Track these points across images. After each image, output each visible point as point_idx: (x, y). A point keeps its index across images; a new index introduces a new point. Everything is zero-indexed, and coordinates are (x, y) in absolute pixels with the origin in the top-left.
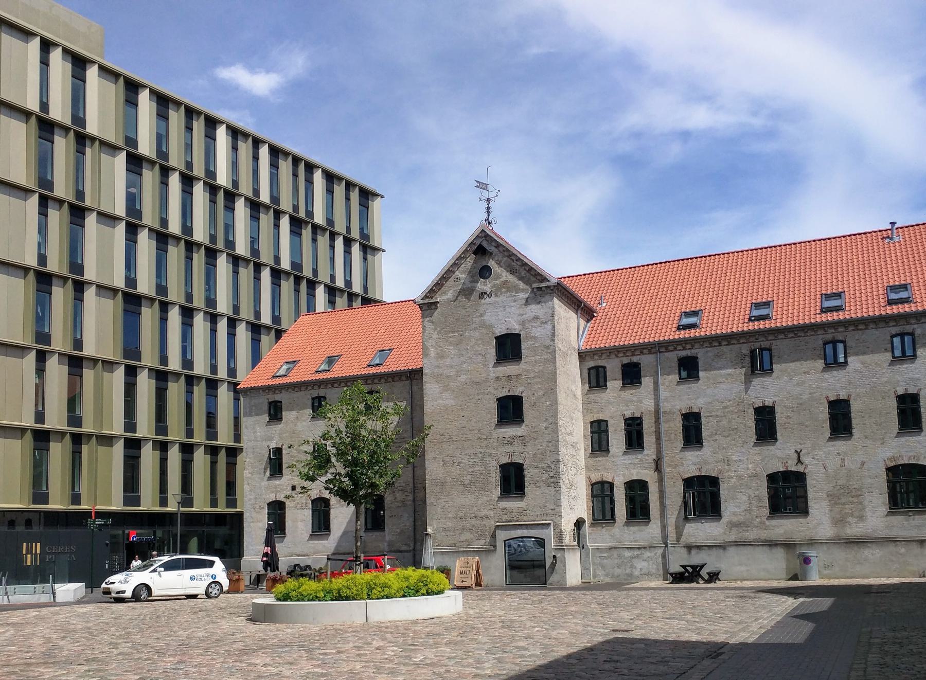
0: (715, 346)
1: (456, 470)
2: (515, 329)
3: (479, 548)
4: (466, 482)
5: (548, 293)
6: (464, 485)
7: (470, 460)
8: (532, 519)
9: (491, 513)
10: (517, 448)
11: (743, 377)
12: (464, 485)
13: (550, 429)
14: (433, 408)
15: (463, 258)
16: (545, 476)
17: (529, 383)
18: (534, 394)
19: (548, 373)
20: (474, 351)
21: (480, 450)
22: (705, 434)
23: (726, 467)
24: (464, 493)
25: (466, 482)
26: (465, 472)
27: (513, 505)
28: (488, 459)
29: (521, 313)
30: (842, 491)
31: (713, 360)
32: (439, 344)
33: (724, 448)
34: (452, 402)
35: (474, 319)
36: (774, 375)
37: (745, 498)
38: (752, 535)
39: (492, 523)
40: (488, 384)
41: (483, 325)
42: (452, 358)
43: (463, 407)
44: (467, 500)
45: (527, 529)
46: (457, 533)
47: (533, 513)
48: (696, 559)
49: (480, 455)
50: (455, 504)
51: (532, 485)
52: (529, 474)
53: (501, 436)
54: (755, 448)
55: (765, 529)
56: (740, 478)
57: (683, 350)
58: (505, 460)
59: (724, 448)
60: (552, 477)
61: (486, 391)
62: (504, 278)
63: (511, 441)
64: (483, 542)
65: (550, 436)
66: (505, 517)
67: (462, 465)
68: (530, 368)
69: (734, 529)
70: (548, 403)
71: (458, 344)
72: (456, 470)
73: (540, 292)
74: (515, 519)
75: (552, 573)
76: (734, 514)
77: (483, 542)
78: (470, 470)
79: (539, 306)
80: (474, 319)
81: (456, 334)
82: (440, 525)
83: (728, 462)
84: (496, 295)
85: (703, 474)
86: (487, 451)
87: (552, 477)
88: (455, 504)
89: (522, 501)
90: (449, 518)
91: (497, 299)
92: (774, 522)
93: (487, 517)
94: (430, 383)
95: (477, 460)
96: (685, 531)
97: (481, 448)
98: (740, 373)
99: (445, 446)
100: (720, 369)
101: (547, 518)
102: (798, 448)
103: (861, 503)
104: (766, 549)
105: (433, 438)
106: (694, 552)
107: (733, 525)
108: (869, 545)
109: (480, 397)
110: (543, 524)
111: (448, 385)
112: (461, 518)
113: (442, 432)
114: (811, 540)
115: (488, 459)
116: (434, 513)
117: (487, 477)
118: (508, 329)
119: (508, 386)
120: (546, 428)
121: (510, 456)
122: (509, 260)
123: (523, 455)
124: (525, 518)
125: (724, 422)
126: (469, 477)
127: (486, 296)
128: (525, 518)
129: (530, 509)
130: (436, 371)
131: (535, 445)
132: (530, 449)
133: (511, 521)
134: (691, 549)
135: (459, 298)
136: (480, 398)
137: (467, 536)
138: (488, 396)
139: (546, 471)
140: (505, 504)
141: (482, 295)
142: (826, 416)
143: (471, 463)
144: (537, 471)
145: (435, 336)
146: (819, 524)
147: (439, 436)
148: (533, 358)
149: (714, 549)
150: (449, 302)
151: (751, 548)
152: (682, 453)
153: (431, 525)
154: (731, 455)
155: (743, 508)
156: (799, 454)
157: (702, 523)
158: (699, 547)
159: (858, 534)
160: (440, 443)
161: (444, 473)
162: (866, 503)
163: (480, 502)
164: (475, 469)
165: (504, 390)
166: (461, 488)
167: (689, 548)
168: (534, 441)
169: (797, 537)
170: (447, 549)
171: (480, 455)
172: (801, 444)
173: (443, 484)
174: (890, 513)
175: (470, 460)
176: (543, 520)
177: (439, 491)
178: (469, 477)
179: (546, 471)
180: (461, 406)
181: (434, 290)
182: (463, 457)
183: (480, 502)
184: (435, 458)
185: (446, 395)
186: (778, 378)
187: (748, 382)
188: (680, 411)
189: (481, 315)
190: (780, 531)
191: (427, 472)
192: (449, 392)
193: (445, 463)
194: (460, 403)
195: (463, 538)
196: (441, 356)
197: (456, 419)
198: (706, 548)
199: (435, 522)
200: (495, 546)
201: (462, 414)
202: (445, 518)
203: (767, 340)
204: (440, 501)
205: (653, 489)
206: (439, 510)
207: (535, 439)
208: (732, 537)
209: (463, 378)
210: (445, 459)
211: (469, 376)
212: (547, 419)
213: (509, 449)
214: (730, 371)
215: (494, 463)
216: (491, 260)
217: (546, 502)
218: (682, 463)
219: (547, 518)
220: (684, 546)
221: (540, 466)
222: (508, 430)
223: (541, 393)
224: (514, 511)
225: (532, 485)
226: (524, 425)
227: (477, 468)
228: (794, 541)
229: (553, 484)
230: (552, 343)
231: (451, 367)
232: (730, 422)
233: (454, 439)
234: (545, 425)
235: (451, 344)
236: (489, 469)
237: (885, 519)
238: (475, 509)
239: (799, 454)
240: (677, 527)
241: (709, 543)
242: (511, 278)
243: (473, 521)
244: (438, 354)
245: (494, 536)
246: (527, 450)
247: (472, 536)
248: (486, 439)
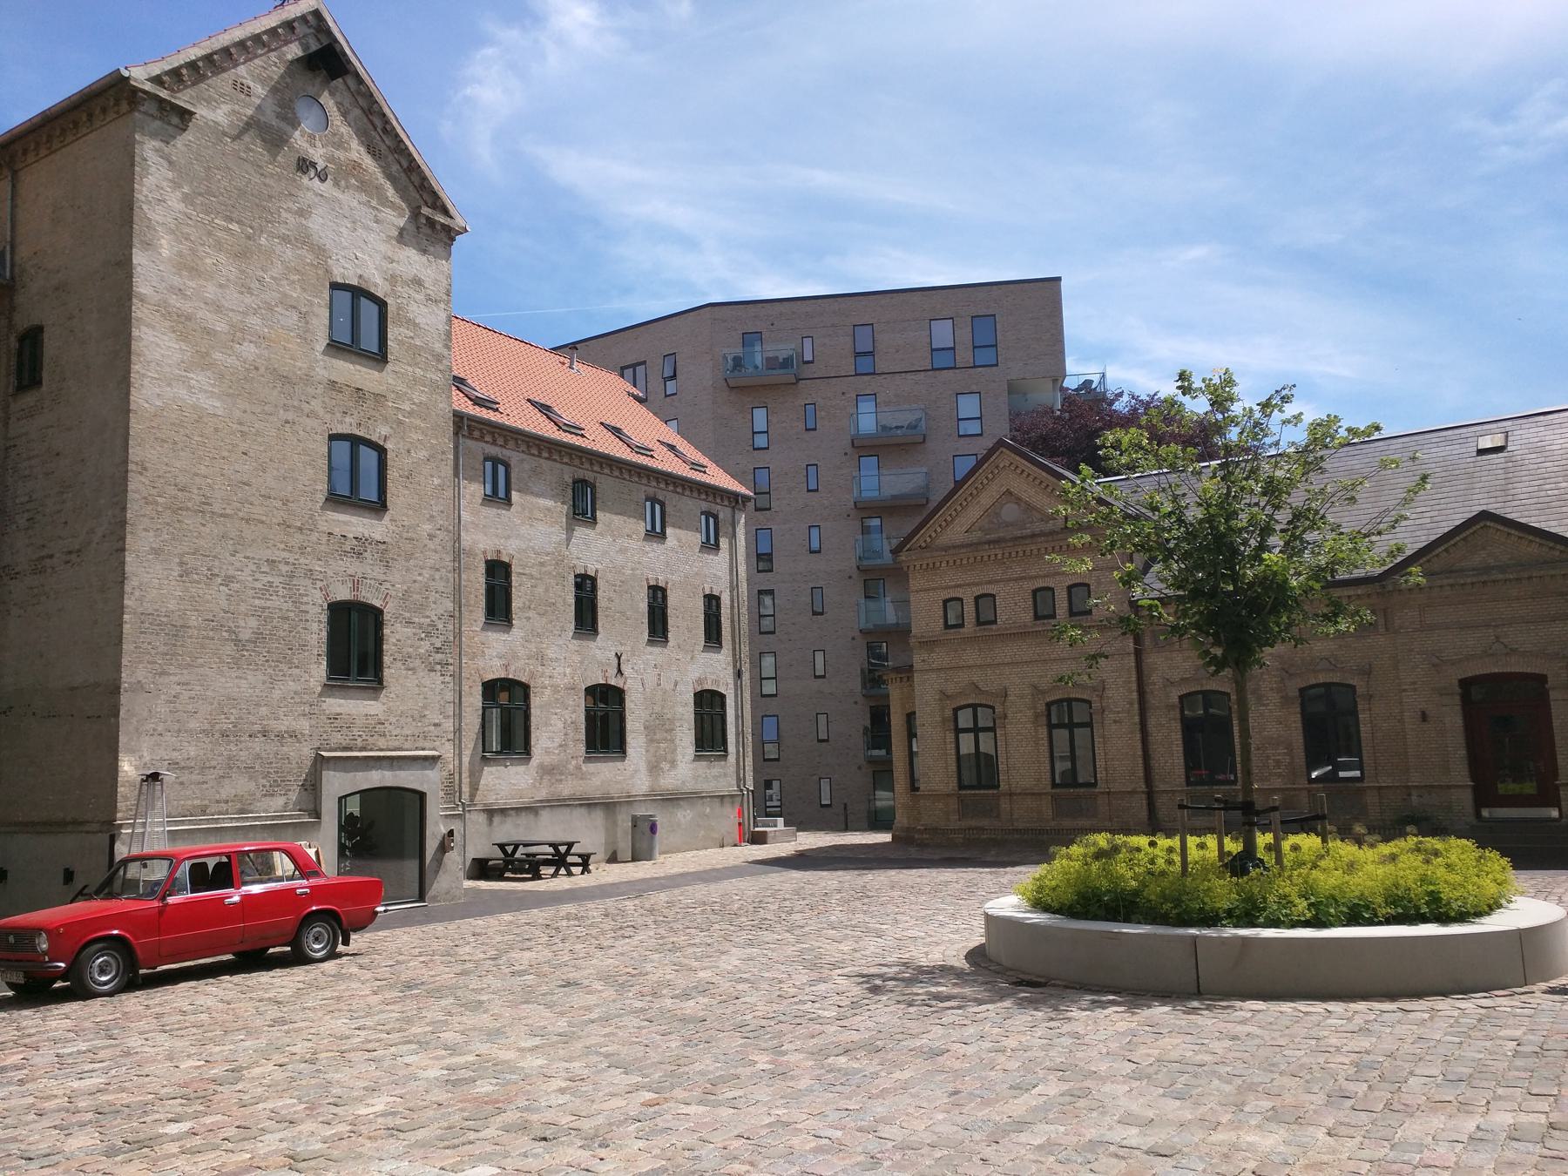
0: (533, 455)
1: (217, 597)
2: (376, 285)
3: (273, 818)
4: (245, 635)
5: (441, 240)
6: (237, 642)
7: (258, 576)
8: (396, 744)
9: (304, 725)
10: (369, 568)
11: (564, 520)
12: (237, 642)
13: (437, 541)
14: (159, 403)
15: (264, 45)
16: (425, 647)
17: (400, 423)
18: (409, 451)
19: (437, 415)
20: (279, 292)
21: (285, 555)
22: (516, 604)
23: (540, 668)
24: (236, 663)
25: (245, 635)
26: (243, 608)
27: (355, 707)
28: (303, 583)
29: (390, 254)
30: (657, 722)
31: (530, 477)
32: (187, 230)
33: (538, 635)
34: (218, 404)
35: (284, 214)
36: (599, 527)
37: (560, 725)
38: (567, 788)
39: (304, 753)
40: (310, 390)
41: (303, 239)
42: (221, 286)
43: (245, 429)
44: (247, 684)
45: (391, 768)
46: (211, 776)
47: (397, 731)
48: (509, 831)
49: (284, 568)
50: (209, 693)
51: (399, 664)
52: (395, 636)
53: (337, 531)
54: (575, 642)
55: (582, 779)
56: (555, 689)
57: (492, 444)
58: (343, 594)
59: (538, 635)
60: (438, 650)
61: (305, 406)
62: (354, 155)
63: (360, 547)
64: (279, 801)
65: (437, 557)
66: (337, 739)
67: (235, 586)
68: (401, 388)
69: (547, 777)
70: (436, 481)
71: (241, 255)
72: (217, 597)
73: (429, 231)
74: (359, 742)
75: (437, 872)
76: (547, 752)
77: (279, 801)
78: (257, 602)
79: (424, 259)
80: (284, 214)
81: (234, 227)
82: (162, 753)
83: (541, 658)
84: (336, 184)
85: (510, 677)
86: (302, 561)
87: (438, 650)
88: (209, 693)
89: (376, 699)
90: (190, 732)
91: (337, 193)
92: (592, 767)
93: (293, 735)
94: (153, 328)
95: (277, 580)
96: (482, 782)
97: (289, 549)
98: (561, 509)
99: (190, 521)
100: (537, 495)
101: (427, 745)
102: (620, 649)
103: (673, 741)
104: (583, 811)
105: (154, 492)
106: (497, 819)
107: (548, 771)
108: (682, 803)
109: (290, 416)
110: (426, 758)
111: (207, 354)
112: (224, 734)
113: (182, 480)
114: (629, 797)
115: (303, 583)
116: (145, 714)
117: (299, 629)
118: (360, 276)
119: (356, 413)
120: (431, 537)
121: (356, 586)
122: (365, 120)
123: (383, 588)
124: (382, 743)
125: (540, 590)
126: (253, 623)
127: (312, 173)
128: (382, 743)
129: (393, 720)
130: (174, 300)
131: (408, 570)
132: (398, 579)
133: (350, 749)
134: (492, 816)
135: (247, 138)
136: (290, 418)
137: (241, 785)
138: (308, 420)
139: (428, 634)
140: (339, 705)
141: (304, 165)
142: (646, 609)
143: (258, 585)
144: (409, 631)
145: (175, 201)
146: (636, 771)
147: (171, 490)
148: (410, 369)
149: (524, 814)
150: (219, 133)
151: (567, 811)
152: (485, 634)
153: (132, 751)
154: (547, 648)
155: (558, 741)
156: (619, 658)
157: (506, 766)
158: (503, 811)
159: (670, 787)
160: (177, 510)
161: (182, 599)
162: (677, 742)
163: (277, 694)
164: (269, 604)
165: (348, 419)
166: (229, 649)
167: (491, 813)
168: (408, 561)
169: (615, 792)
170: (182, 822)
171: (284, 568)
172: (621, 644)
173: (177, 631)
174: (697, 758)
175: (258, 576)
176: (417, 749)
177: (162, 649)
178: (253, 623)
179: (428, 634)
180: (240, 424)
181: (181, 75)
182: (238, 565)
183: (277, 694)
184: (156, 552)
185: (200, 378)
186: (601, 534)
187: (570, 530)
188: (484, 552)
189: (302, 213)
190: (596, 781)
191: (127, 589)
192: (209, 373)
193: (184, 574)
194: (237, 414)
195: (227, 791)
196: (188, 266)
197: (226, 454)
198: (513, 812)
199: (145, 745)
200: (317, 814)
201: (243, 446)
202: (179, 731)
203: (592, 471)
204: (166, 679)
205: (730, 702)
206: (162, 709)
207: (410, 556)
208: (542, 794)
209: (249, 350)
210: (187, 558)
211: (266, 353)
212: (432, 516)
213: (354, 567)
214: (549, 503)
215: (318, 597)
216: (326, 93)
217: (425, 707)
218: (483, 652)
219: (427, 745)
220: (483, 810)
221: (417, 620)
222: (354, 519)
223: (423, 454)
224: (357, 721)
225: (399, 664)
226: (387, 517)
227: (276, 602)
228: (612, 798)
229: (439, 667)
230: (445, 352)
231: (218, 308)
232: (547, 590)
233: (217, 508)
234: (427, 527)
235: (219, 246)
236: (303, 608)
237: (691, 766)
238: (264, 711)
239: (619, 658)
240: (472, 774)
241: (513, 802)
242: (368, 162)
243: (258, 745)
244: (180, 254)
245: (312, 787)
246: (390, 578)
247: (252, 786)
248: (300, 529)
